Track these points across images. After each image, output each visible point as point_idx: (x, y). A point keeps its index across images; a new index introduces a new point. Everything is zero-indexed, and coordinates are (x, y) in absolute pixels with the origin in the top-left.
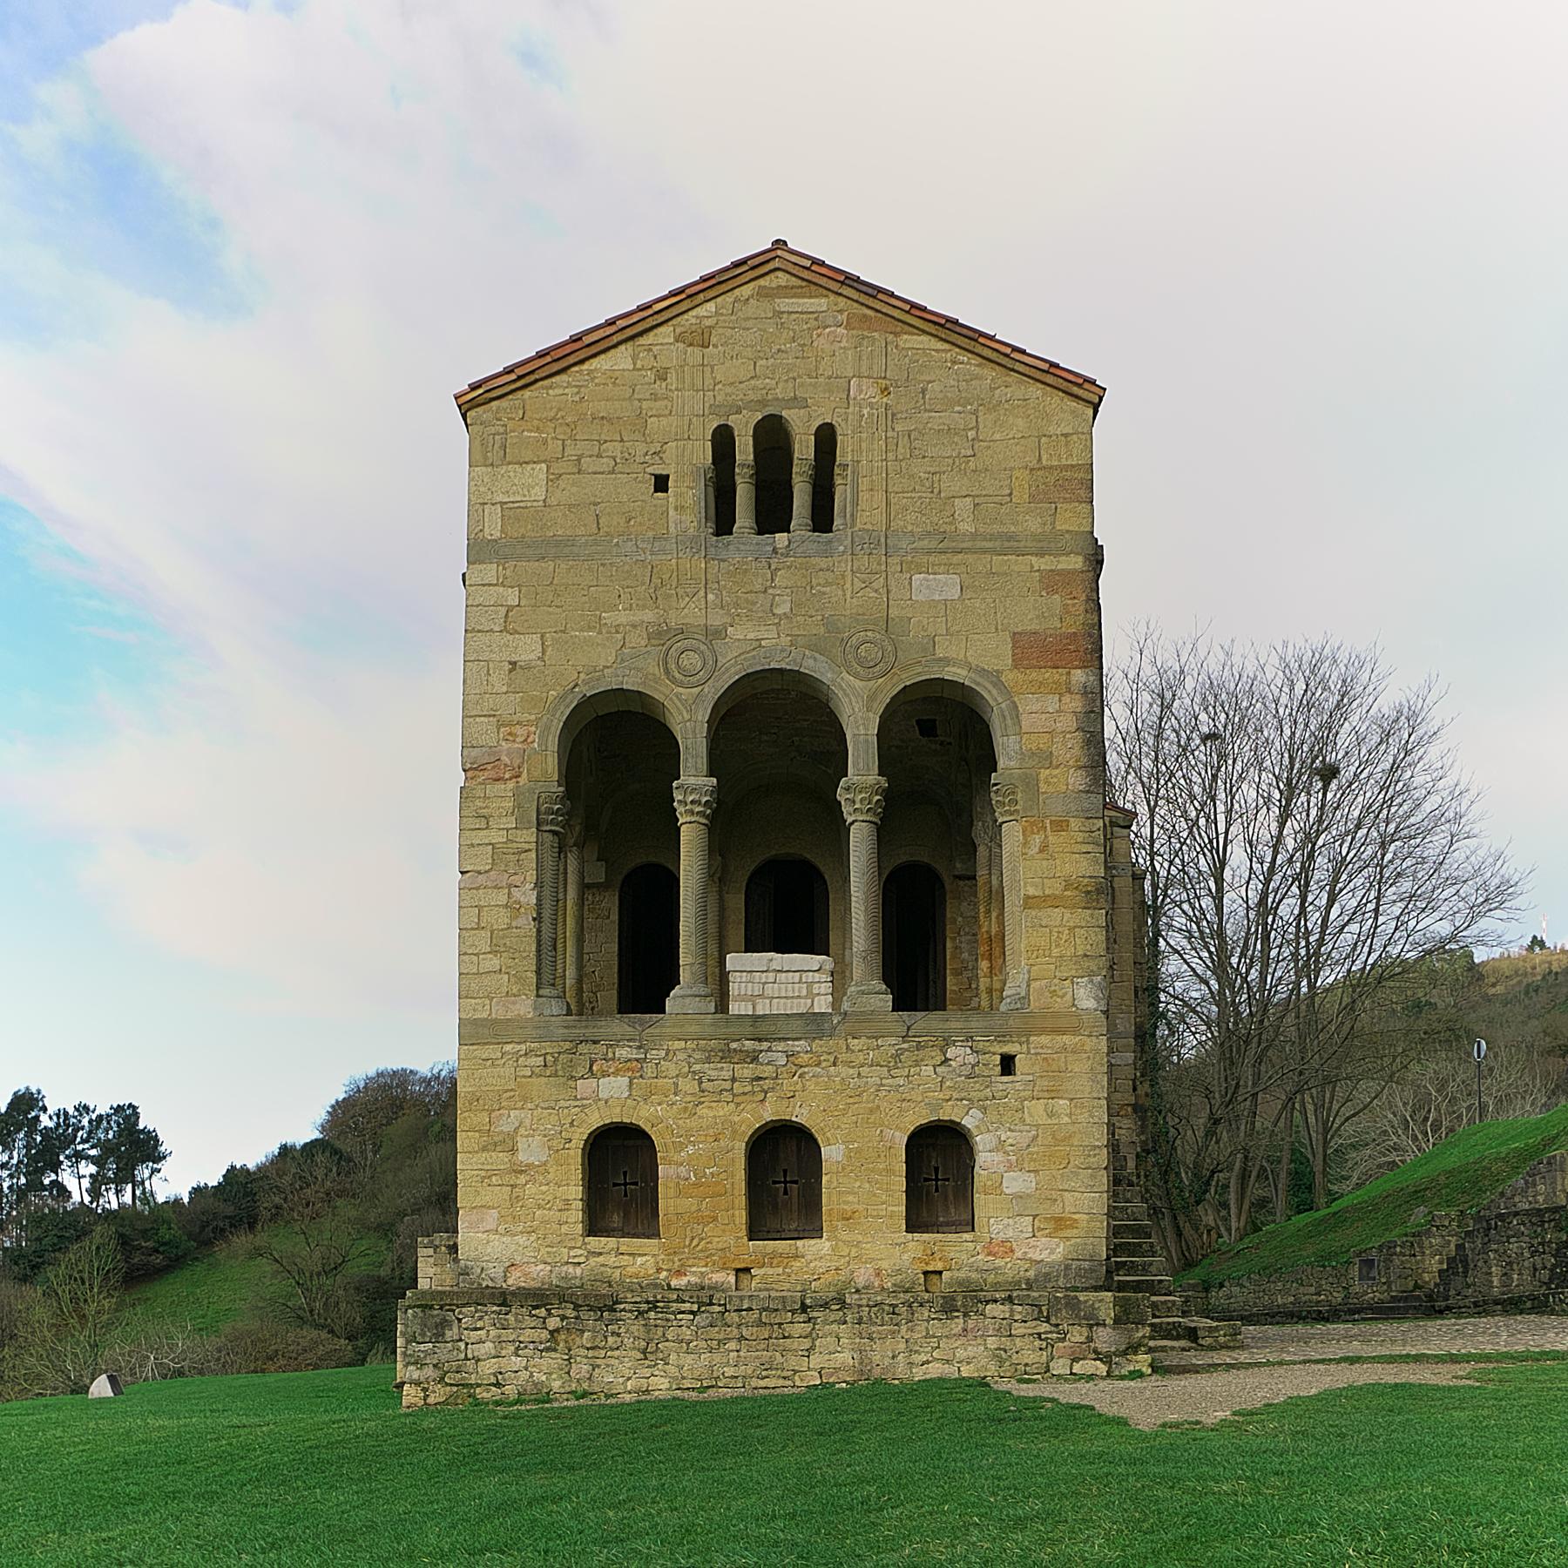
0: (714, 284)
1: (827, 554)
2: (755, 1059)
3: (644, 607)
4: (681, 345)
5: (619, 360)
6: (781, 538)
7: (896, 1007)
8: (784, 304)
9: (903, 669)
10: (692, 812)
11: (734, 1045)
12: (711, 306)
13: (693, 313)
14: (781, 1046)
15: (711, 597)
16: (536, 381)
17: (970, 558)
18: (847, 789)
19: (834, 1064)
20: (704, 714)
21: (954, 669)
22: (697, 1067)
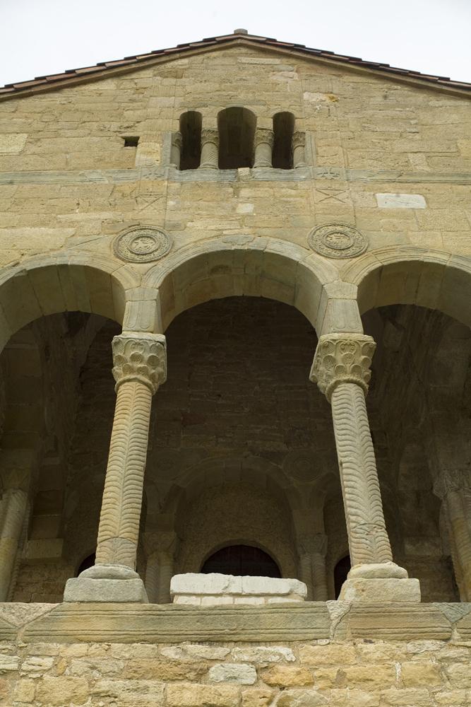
0: (185, 50)
1: (288, 180)
2: (201, 675)
3: (102, 210)
4: (159, 78)
5: (108, 86)
6: (243, 171)
7: (425, 599)
8: (244, 60)
9: (376, 254)
10: (131, 370)
11: (170, 652)
12: (186, 61)
13: (172, 63)
14: (247, 653)
15: (171, 203)
16: (31, 95)
17: (431, 186)
18: (326, 347)
19: (341, 680)
20: (154, 283)
21: (431, 255)
22: (104, 685)
